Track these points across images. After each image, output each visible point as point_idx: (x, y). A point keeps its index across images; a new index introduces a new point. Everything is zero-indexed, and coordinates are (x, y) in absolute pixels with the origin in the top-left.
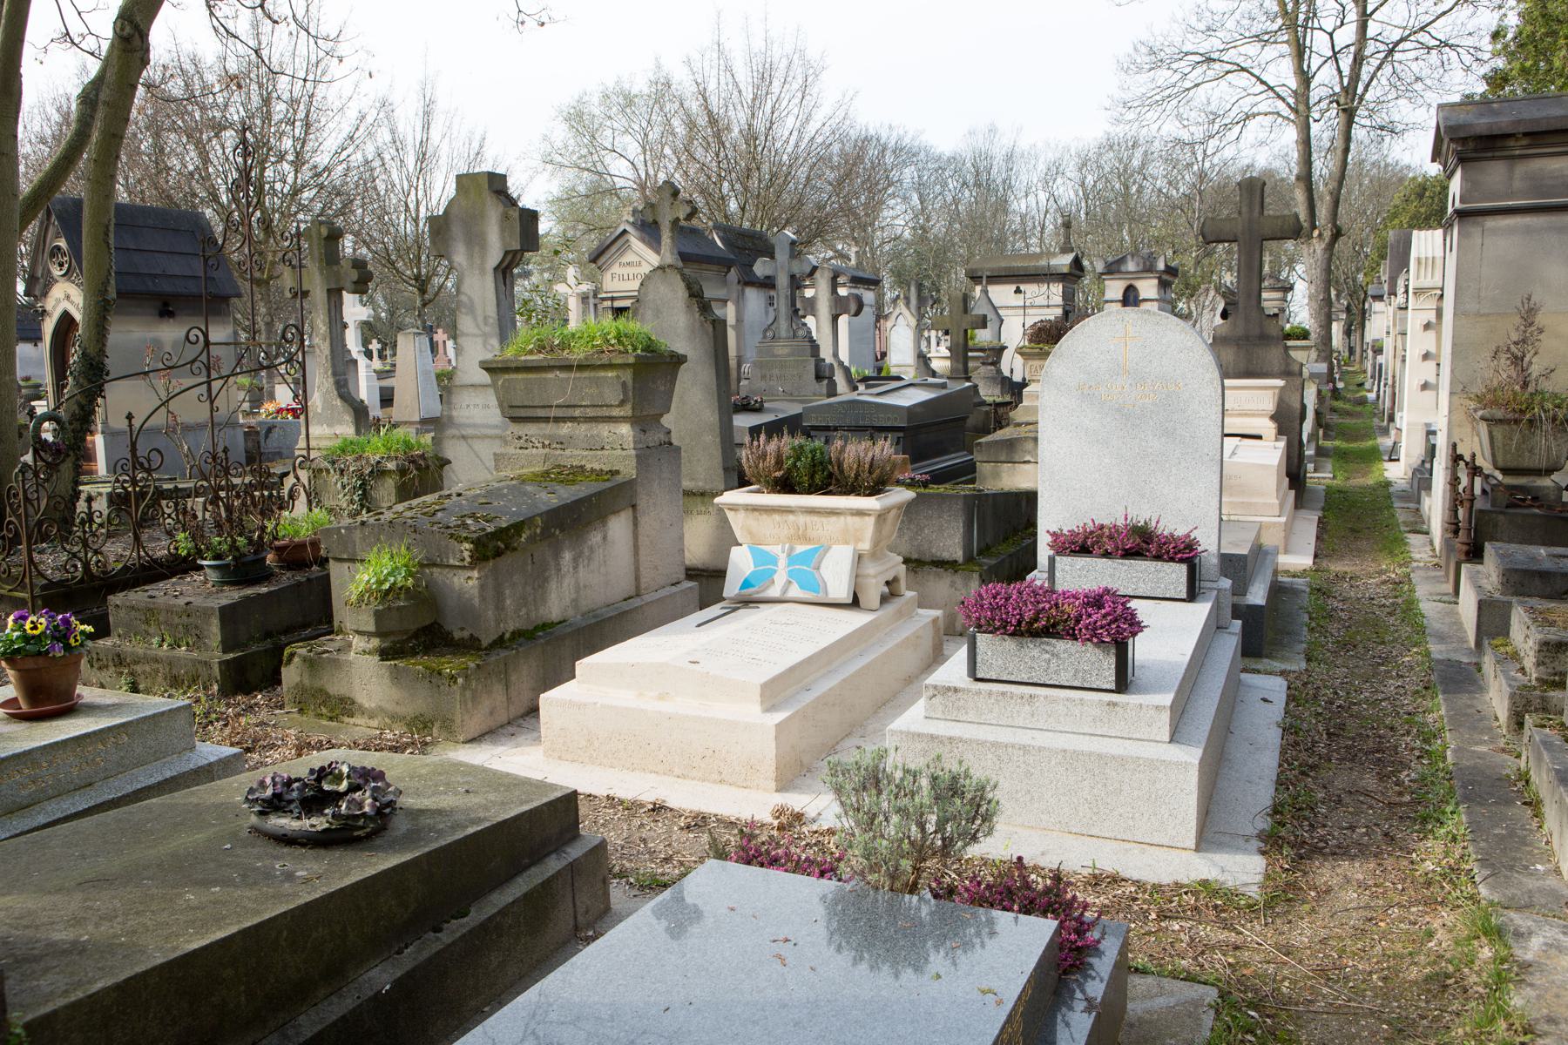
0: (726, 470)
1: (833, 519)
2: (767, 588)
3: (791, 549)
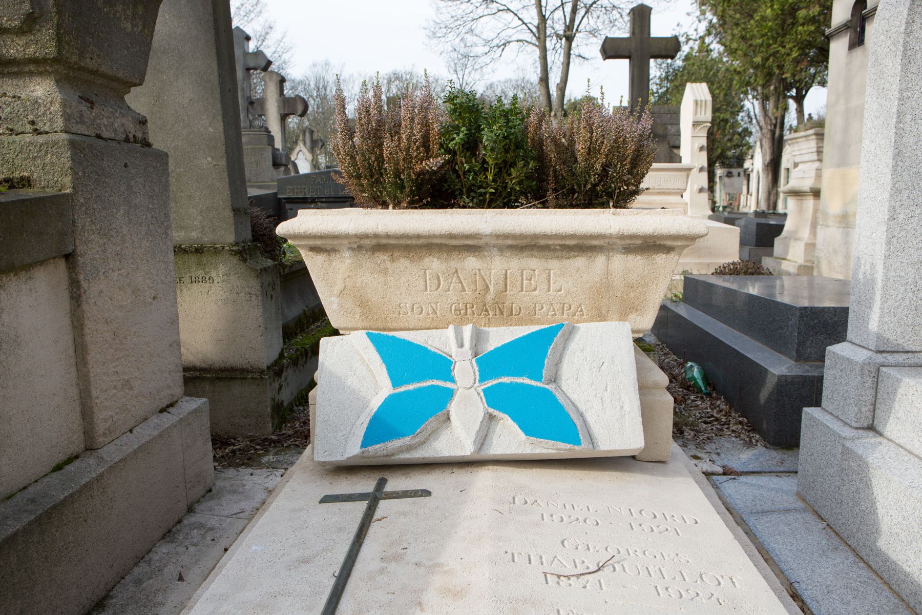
0: (236, 211)
1: (579, 262)
2: (434, 434)
3: (478, 338)
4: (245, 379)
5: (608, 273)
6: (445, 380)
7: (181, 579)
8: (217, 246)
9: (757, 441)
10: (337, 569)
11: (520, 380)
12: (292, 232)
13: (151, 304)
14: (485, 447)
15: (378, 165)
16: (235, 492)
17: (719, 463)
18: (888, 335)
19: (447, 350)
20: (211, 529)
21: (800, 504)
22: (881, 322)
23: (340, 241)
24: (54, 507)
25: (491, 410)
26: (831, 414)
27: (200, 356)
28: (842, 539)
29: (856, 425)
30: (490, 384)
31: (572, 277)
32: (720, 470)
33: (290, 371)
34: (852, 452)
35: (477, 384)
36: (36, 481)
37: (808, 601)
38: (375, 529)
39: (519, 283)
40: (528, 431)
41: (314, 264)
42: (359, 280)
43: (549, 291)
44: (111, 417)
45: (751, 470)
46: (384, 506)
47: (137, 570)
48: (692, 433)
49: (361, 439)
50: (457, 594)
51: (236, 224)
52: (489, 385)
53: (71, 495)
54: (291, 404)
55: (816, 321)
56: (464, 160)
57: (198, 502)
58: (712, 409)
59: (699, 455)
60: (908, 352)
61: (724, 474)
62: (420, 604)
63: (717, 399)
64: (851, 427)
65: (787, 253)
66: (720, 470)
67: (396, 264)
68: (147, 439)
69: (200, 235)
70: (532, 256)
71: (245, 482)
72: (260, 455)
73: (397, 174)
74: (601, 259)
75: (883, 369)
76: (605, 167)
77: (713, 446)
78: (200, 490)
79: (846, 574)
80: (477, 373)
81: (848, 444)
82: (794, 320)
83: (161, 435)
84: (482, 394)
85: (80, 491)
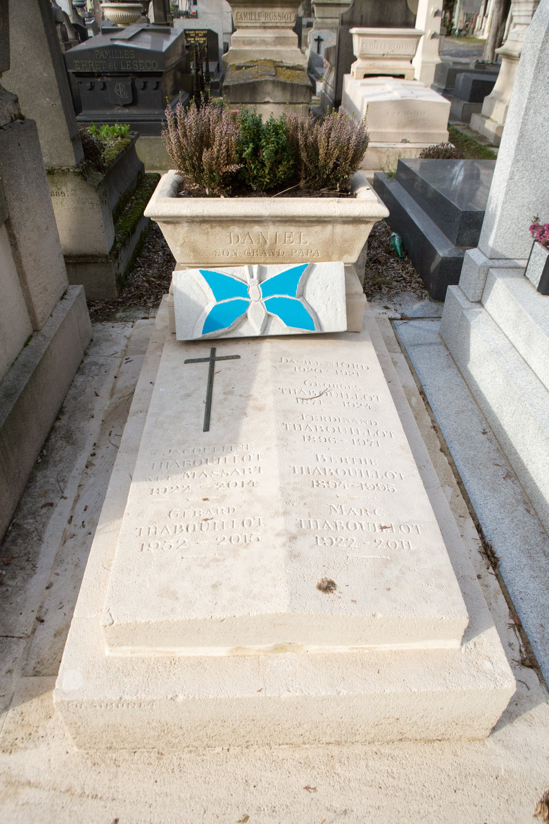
0: (73, 140)
1: (317, 228)
2: (239, 325)
3: (262, 272)
4: (96, 263)
5: (333, 234)
6: (244, 296)
7: (97, 395)
8: (64, 168)
9: (426, 296)
10: (204, 399)
12: (154, 215)
13: (46, 234)
14: (266, 331)
15: (198, 163)
16: (107, 340)
17: (400, 311)
18: (498, 249)
19: (244, 279)
20: (102, 365)
21: (439, 340)
22: (495, 242)
23: (181, 219)
24: (36, 368)
25: (269, 313)
26: (462, 290)
28: (454, 361)
29: (471, 300)
30: (268, 298)
31: (313, 237)
32: (399, 316)
33: (122, 251)
35: (261, 298)
37: (427, 395)
38: (216, 378)
39: (284, 239)
40: (288, 324)
41: (166, 230)
42: (193, 238)
43: (300, 243)
44: (42, 310)
46: (217, 363)
48: (387, 289)
49: (202, 329)
50: (260, 409)
51: (75, 151)
52: (268, 299)
53: (41, 360)
54: (125, 273)
55: (471, 220)
56: (251, 161)
58: (403, 271)
59: (389, 306)
60: (507, 259)
61: (401, 319)
62: (245, 414)
63: (408, 262)
64: (469, 301)
65: (491, 113)
67: (214, 230)
68: (62, 319)
69: (49, 160)
70: (291, 225)
71: (111, 333)
72: (114, 313)
73: (211, 171)
74: (329, 227)
75: (491, 270)
76: (336, 166)
77: (398, 299)
78: (88, 340)
79: (451, 380)
80: (261, 293)
81: (465, 312)
82: (458, 219)
83: (67, 316)
84: (264, 304)
85: (43, 357)
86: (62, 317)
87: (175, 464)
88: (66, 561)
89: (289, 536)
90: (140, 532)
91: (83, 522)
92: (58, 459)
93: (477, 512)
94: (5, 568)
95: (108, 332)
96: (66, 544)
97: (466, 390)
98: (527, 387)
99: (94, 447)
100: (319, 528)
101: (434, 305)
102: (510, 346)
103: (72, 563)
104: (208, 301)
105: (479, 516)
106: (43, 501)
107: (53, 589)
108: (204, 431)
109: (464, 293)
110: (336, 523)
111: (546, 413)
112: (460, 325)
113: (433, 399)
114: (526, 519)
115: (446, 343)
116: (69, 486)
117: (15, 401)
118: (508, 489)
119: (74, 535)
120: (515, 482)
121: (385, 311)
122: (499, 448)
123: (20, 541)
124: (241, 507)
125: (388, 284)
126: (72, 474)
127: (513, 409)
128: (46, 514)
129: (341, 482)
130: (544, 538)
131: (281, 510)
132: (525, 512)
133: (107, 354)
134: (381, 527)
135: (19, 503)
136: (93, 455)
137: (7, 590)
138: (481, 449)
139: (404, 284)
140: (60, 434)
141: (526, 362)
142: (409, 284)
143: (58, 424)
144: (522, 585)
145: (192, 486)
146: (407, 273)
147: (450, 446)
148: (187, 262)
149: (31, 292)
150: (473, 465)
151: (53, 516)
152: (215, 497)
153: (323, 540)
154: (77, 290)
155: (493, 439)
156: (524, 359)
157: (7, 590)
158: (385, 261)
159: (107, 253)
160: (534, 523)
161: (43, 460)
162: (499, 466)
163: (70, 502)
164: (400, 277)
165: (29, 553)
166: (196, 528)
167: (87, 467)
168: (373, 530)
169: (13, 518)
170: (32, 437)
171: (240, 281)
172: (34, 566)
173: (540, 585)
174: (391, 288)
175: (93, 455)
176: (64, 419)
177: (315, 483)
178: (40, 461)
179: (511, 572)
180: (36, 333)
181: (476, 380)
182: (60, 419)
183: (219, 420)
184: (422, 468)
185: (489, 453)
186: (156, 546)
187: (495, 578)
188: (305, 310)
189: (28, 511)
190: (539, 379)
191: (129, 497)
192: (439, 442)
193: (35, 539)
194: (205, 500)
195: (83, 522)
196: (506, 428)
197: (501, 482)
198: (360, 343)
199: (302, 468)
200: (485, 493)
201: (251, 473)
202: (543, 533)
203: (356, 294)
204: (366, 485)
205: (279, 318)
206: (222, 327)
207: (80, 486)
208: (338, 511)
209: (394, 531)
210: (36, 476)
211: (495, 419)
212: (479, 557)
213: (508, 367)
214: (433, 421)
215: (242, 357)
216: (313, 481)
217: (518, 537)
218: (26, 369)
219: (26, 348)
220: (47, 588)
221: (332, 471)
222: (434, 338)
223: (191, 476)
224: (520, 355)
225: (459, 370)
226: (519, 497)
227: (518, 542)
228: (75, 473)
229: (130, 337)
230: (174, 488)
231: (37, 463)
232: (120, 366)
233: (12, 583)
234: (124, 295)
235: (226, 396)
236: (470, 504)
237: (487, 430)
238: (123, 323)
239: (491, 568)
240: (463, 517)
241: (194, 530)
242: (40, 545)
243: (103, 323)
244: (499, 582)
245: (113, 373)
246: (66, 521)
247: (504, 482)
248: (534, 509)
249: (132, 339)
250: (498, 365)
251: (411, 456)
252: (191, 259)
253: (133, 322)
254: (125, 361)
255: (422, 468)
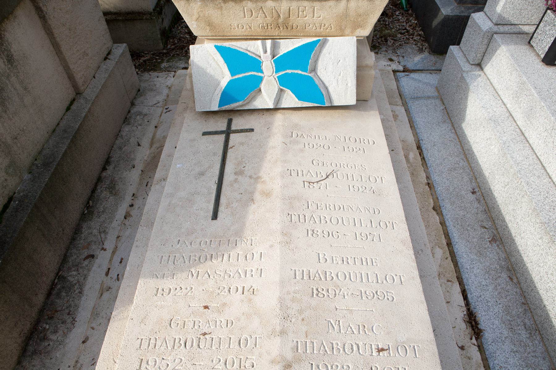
2: (254, 98)
3: (275, 47)
4: (142, 19)
5: (347, 8)
6: (258, 71)
7: (139, 145)
9: (426, 48)
10: (216, 179)
11: (296, 71)
14: (279, 104)
16: (152, 90)
17: (402, 64)
19: (258, 53)
20: (146, 115)
21: (436, 94)
22: (504, 8)
24: (76, 133)
25: (281, 87)
26: (463, 52)
27: (112, 5)
28: (449, 116)
29: (471, 62)
30: (281, 73)
32: (401, 68)
33: (166, 7)
34: (465, 80)
35: (274, 74)
36: (62, 119)
37: (424, 150)
39: (297, 13)
42: (207, 13)
43: (313, 17)
44: (83, 75)
45: (418, 69)
46: (233, 136)
47: (118, 142)
48: (392, 41)
50: (267, 194)
52: (281, 74)
53: (81, 124)
54: (170, 26)
57: (135, 98)
58: (406, 23)
59: (393, 58)
60: (512, 25)
61: (404, 71)
62: (253, 200)
63: (411, 15)
64: (469, 63)
66: (401, 68)
67: (226, 5)
68: (104, 80)
72: (159, 63)
75: (495, 36)
79: (445, 136)
80: (274, 68)
81: (465, 75)
83: (110, 76)
84: (277, 79)
85: (83, 121)
86: (104, 78)
87: (182, 259)
88: (101, 315)
89: (284, 363)
90: (141, 343)
91: (118, 275)
92: (101, 209)
93: (464, 277)
94: (49, 321)
95: (153, 82)
96: (102, 297)
97: (459, 147)
98: (524, 163)
99: (133, 198)
100: (315, 352)
101: (433, 58)
102: (507, 114)
103: (106, 317)
104: (224, 77)
105: (465, 281)
106: (86, 253)
107: (88, 343)
108: (212, 219)
109: (465, 55)
110: (332, 344)
111: (542, 194)
112: (458, 86)
113: (429, 155)
114: (508, 287)
115: (443, 98)
116: (109, 237)
117: (52, 170)
118: (493, 254)
119: (110, 288)
120: (500, 246)
121: (390, 63)
122: (487, 209)
123: (63, 294)
124: (239, 321)
125: (393, 36)
126: (113, 225)
127: (507, 181)
128: (87, 266)
129: (341, 290)
130: (525, 310)
131: (278, 328)
132: (508, 279)
133: (151, 104)
134: (378, 349)
135: (65, 255)
136: (132, 206)
137: (49, 345)
138: (470, 210)
139: (407, 36)
140: (105, 184)
141: (523, 134)
142: (411, 36)
143: (104, 174)
144: (502, 360)
145: (195, 289)
146: (411, 26)
147: (442, 205)
148: (204, 35)
149: (68, 60)
150: (462, 226)
151: (93, 268)
152: (215, 305)
153: (318, 368)
154: (121, 49)
155: (481, 199)
156: (521, 130)
157: (49, 345)
158: (392, 13)
159: (152, 10)
160: (516, 292)
161: (89, 210)
162: (486, 228)
163: (108, 253)
164: (404, 30)
165: (70, 306)
166: (194, 344)
167: (125, 218)
168: (370, 354)
169: (60, 270)
170: (76, 194)
171: (254, 56)
172: (74, 320)
173: (520, 361)
174: (395, 40)
175: (132, 206)
176: (110, 168)
177: (315, 292)
178: (86, 212)
179: (493, 344)
180: (78, 96)
181: (470, 140)
182: (106, 169)
183: (228, 206)
184: (420, 252)
185: (477, 214)
186: (154, 363)
187: (477, 349)
188: (317, 86)
189: (73, 263)
190: (536, 154)
191: (135, 298)
192: (432, 200)
193: (77, 291)
194: (206, 307)
195: (118, 275)
196: (496, 194)
197: (486, 246)
198: (367, 113)
199: (303, 271)
200: (472, 257)
201: (252, 275)
202: (524, 304)
203: (367, 66)
204: (365, 292)
205: (291, 93)
206: (236, 101)
207: (118, 237)
208: (335, 327)
209: (392, 355)
210: (82, 227)
211: (485, 182)
212: (463, 326)
213: (504, 139)
214: (428, 178)
215: (255, 131)
216: (313, 289)
217: (501, 306)
218: (66, 135)
219: (69, 113)
220: (84, 342)
221: (332, 275)
222: (431, 92)
223: (195, 275)
224: (518, 125)
225: (453, 126)
226: (503, 263)
227: (501, 311)
228: (115, 224)
229: (171, 86)
230: (178, 289)
231: (83, 214)
232: (161, 116)
233: (53, 337)
234: (169, 47)
235: (236, 177)
236: (457, 268)
237: (476, 190)
238: (167, 73)
239: (474, 338)
240: (451, 281)
241: (192, 345)
242: (81, 297)
243: (150, 73)
244: (481, 354)
245: (154, 123)
246: (104, 273)
247: (490, 246)
248: (517, 278)
249: (173, 89)
250: (495, 135)
251: (412, 252)
252: (208, 32)
253: (175, 72)
254: (165, 111)
255: (420, 252)
